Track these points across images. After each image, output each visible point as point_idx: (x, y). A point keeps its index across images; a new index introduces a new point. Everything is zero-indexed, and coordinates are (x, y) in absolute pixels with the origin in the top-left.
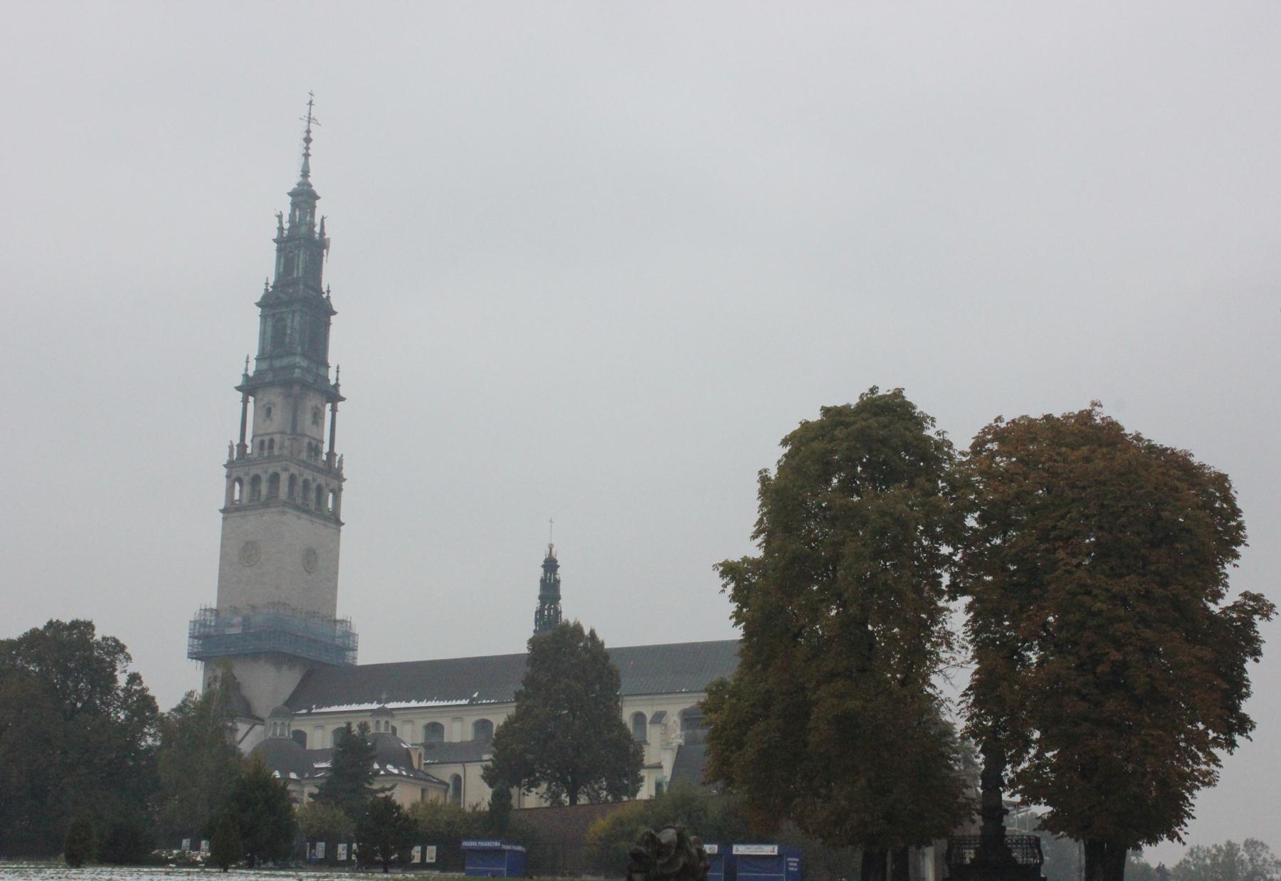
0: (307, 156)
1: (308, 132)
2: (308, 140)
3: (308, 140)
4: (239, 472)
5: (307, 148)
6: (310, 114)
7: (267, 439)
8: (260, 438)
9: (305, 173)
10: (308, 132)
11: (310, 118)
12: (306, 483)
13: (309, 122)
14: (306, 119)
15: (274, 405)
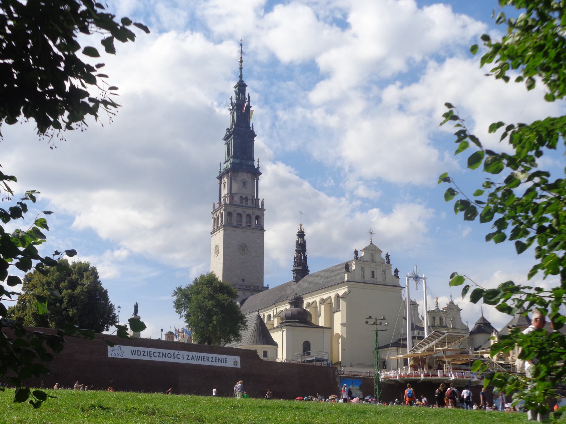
0: (241, 68)
1: (241, 58)
2: (241, 62)
3: (241, 62)
4: (231, 209)
5: (241, 65)
6: (241, 50)
7: (244, 196)
8: (240, 195)
9: (241, 77)
10: (241, 58)
11: (241, 51)
12: (249, 216)
13: (241, 53)
14: (240, 52)
15: (247, 181)
